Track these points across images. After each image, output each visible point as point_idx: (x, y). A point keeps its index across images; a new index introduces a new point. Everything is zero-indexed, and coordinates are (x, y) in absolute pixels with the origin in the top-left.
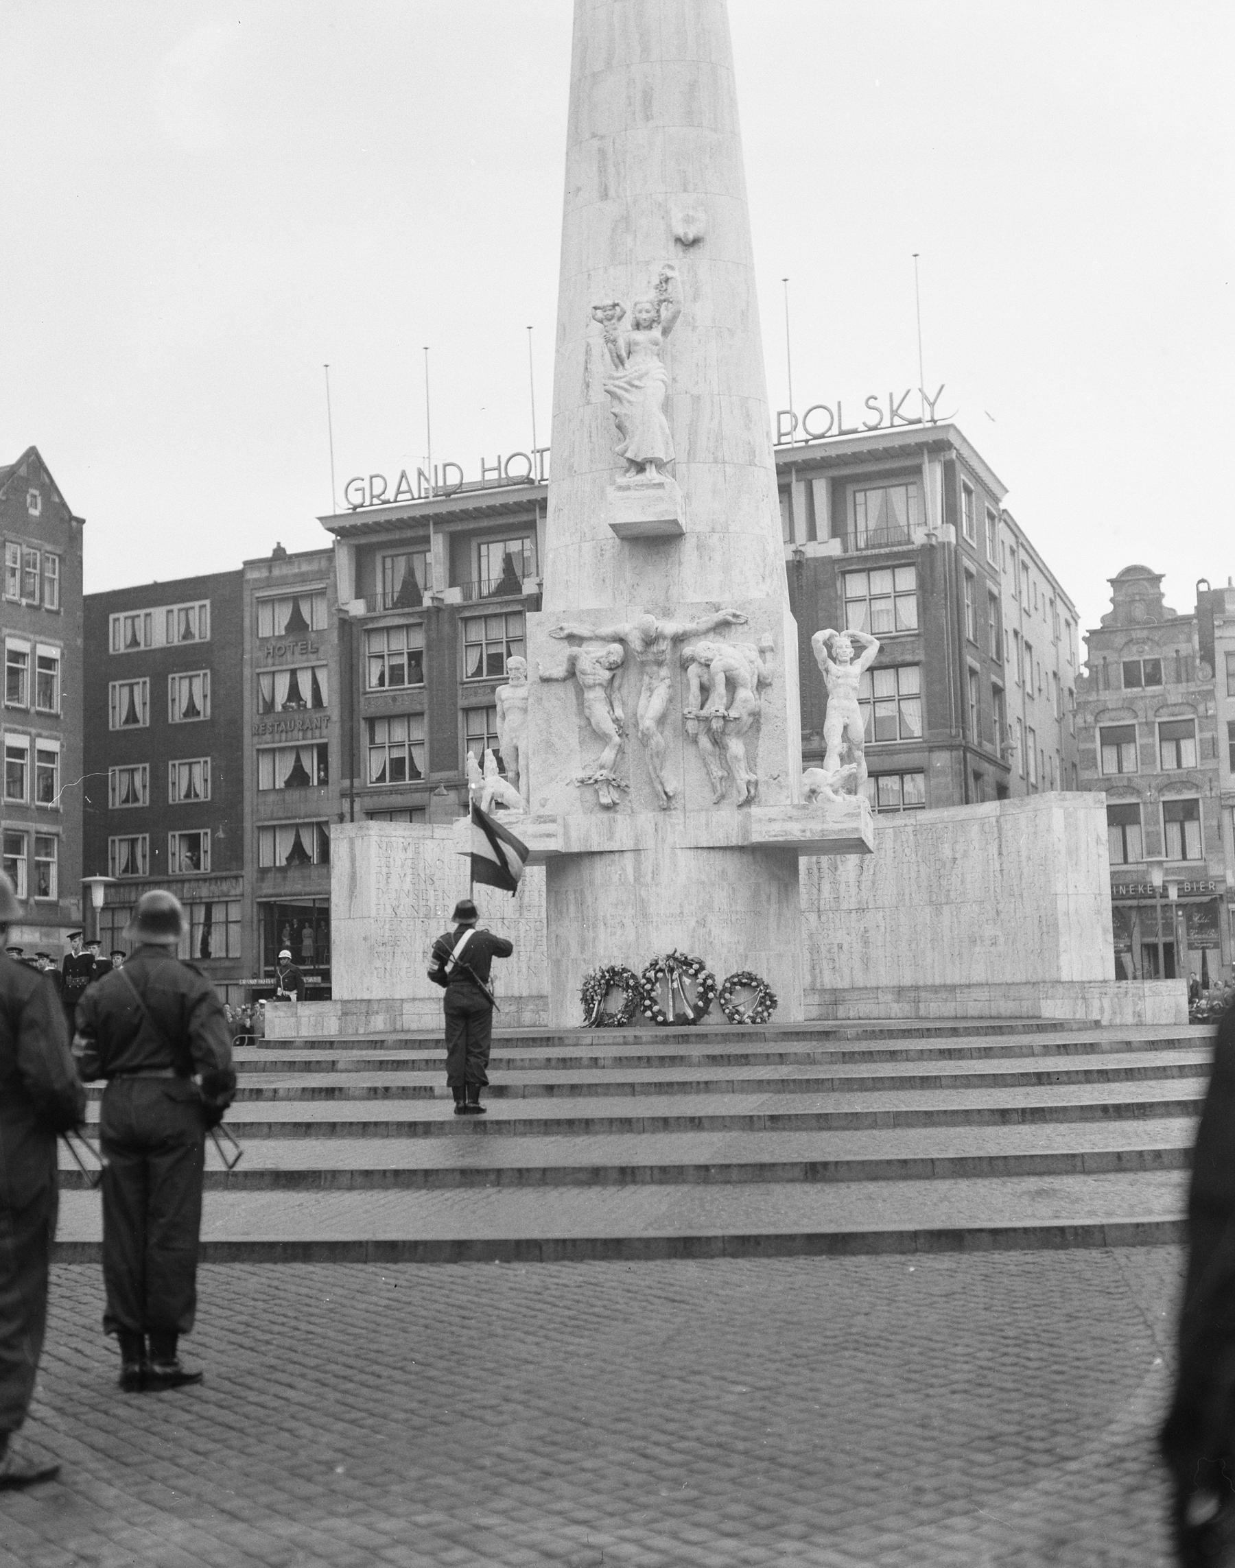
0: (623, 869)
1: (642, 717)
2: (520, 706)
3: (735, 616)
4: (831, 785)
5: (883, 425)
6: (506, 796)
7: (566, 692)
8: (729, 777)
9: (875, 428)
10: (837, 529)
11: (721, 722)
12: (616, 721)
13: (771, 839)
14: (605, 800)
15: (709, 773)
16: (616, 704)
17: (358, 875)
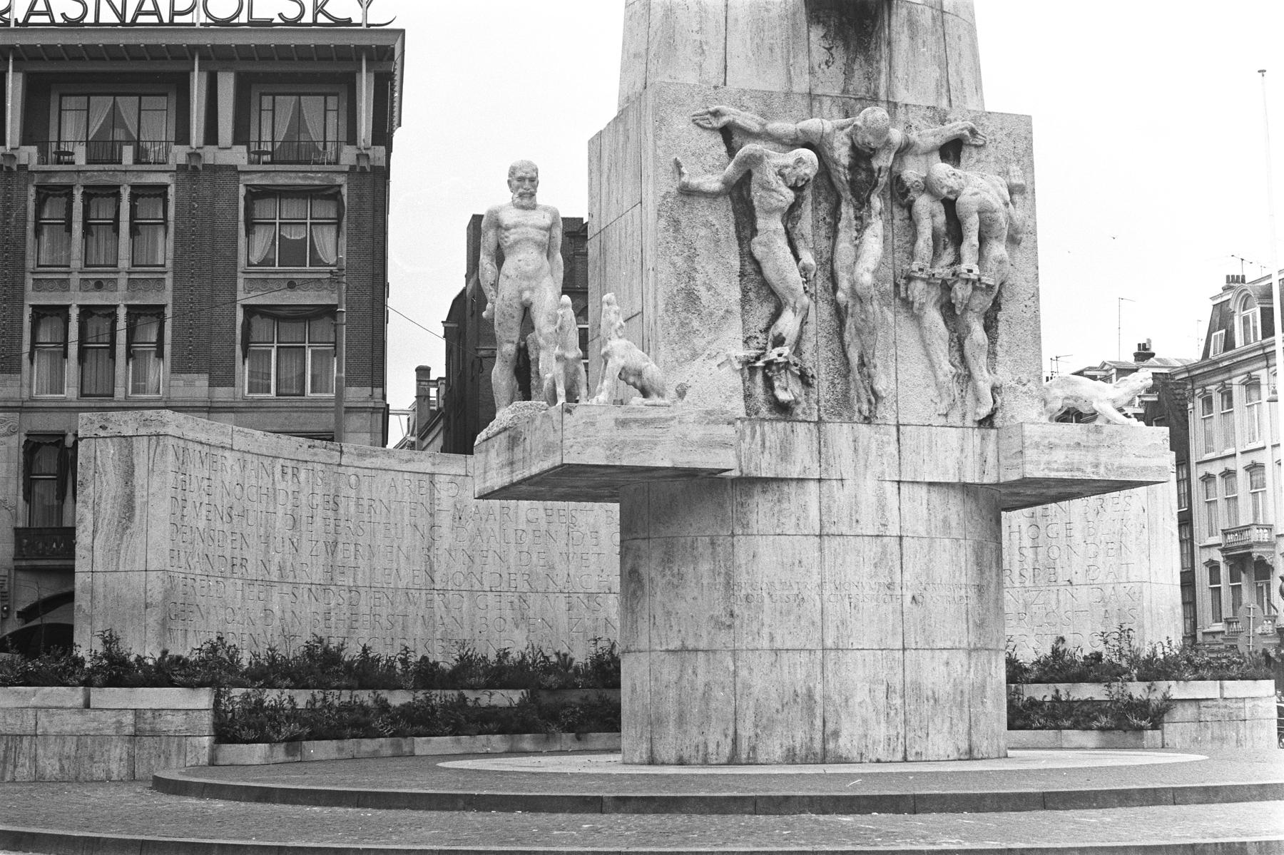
0: (804, 508)
1: (851, 269)
2: (539, 238)
3: (973, 132)
4: (1114, 401)
5: (303, 20)
6: (645, 376)
7: (722, 219)
8: (966, 377)
9: (294, 22)
10: (241, 136)
11: (970, 287)
12: (804, 271)
13: (1053, 475)
14: (783, 396)
15: (932, 366)
16: (800, 244)
17: (138, 502)
